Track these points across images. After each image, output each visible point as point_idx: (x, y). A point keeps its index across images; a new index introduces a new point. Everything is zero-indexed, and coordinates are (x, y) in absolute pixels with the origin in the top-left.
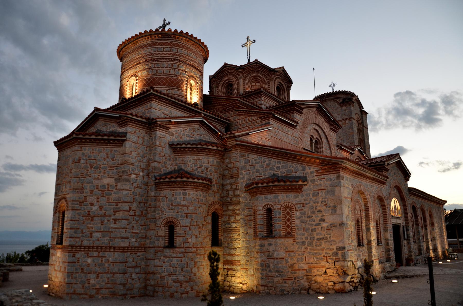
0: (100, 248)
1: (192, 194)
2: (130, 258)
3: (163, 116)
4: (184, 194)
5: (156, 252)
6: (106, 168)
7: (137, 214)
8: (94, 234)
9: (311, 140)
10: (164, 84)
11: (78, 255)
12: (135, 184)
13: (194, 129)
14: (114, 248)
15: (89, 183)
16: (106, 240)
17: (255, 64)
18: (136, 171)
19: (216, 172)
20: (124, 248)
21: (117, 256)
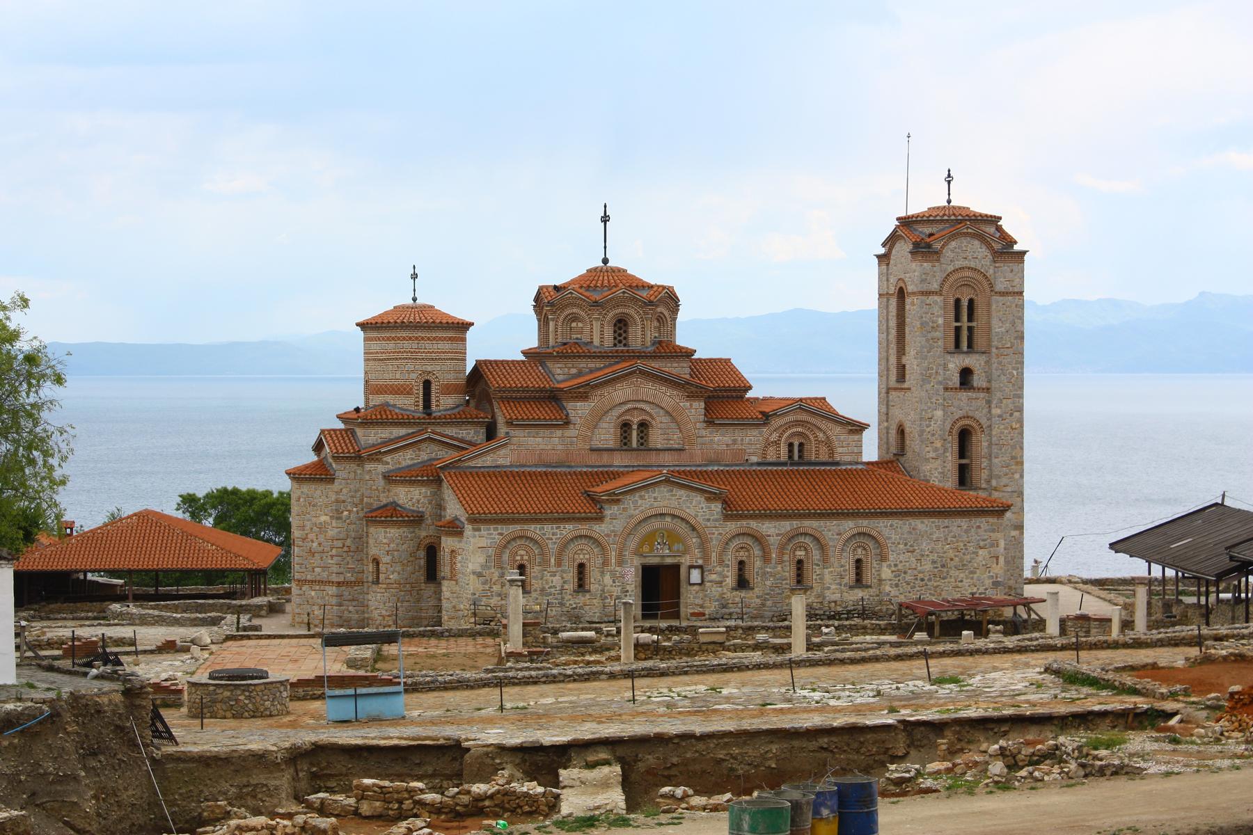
0: (321, 582)
1: (394, 532)
2: (346, 592)
3: (379, 441)
4: (386, 532)
5: (369, 587)
6: (321, 505)
7: (352, 549)
8: (316, 569)
9: (626, 426)
10: (391, 393)
11: (304, 588)
12: (348, 521)
13: (419, 449)
14: (333, 582)
15: (308, 521)
16: (325, 575)
17: (570, 295)
18: (349, 508)
19: (429, 503)
20: (339, 583)
21: (332, 590)
